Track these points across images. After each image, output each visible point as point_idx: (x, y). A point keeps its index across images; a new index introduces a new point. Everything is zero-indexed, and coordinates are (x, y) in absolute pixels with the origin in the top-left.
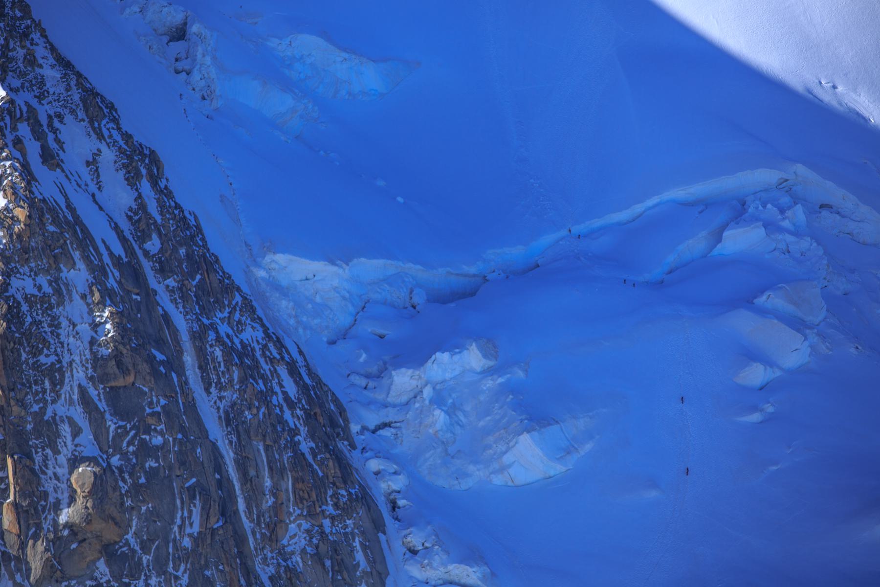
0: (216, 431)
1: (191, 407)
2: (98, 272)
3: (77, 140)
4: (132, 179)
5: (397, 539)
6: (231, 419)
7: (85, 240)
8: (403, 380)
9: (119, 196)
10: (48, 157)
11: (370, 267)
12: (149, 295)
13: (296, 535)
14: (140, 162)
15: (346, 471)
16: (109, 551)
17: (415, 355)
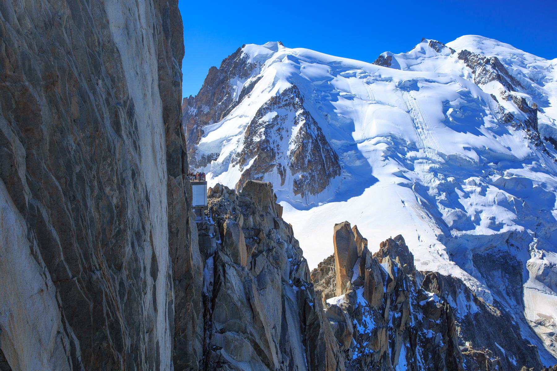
0: (323, 158)
1: (321, 155)
2: (313, 140)
3: (312, 126)
4: (318, 131)
5: (342, 170)
6: (325, 157)
7: (312, 137)
8: (345, 154)
9: (316, 133)
10: (309, 128)
11: (343, 142)
12: (318, 143)
13: (331, 169)
14: (319, 129)
15: (337, 163)
16: (311, 169)
17: (347, 151)
